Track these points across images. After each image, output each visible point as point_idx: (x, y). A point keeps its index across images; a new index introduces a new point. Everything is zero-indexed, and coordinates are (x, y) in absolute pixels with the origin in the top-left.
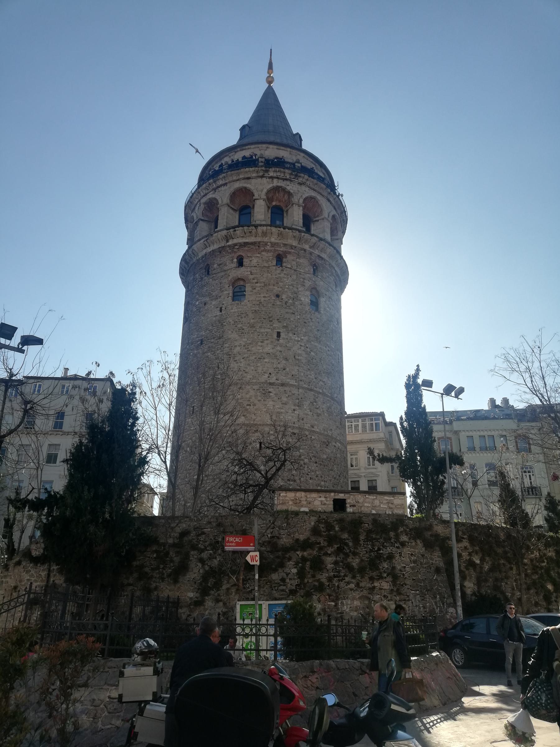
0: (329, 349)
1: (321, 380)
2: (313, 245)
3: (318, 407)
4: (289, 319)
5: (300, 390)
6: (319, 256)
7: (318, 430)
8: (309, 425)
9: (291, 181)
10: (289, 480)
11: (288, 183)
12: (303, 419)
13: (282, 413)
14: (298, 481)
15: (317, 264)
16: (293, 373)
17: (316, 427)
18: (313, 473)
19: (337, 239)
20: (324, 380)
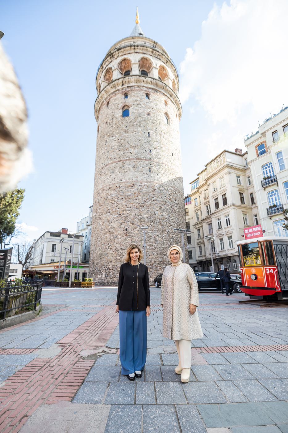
0: (136, 133)
1: (127, 153)
2: (122, 84)
3: (125, 168)
4: (110, 130)
5: (114, 164)
6: (128, 87)
7: (124, 181)
8: (119, 180)
9: (112, 61)
10: (107, 213)
11: (111, 63)
12: (114, 179)
13: (105, 180)
14: (111, 212)
15: (127, 92)
16: (111, 157)
17: (123, 180)
18: (120, 205)
19: (152, 68)
20: (131, 151)
